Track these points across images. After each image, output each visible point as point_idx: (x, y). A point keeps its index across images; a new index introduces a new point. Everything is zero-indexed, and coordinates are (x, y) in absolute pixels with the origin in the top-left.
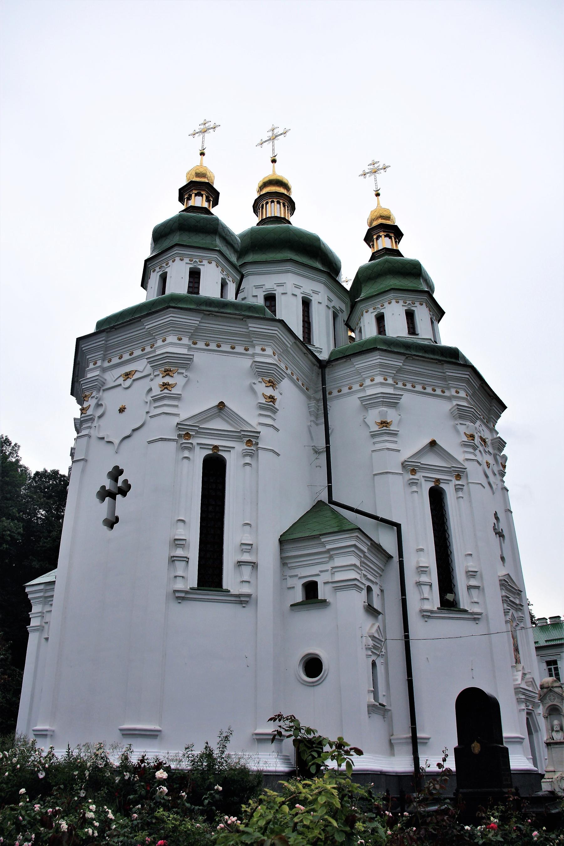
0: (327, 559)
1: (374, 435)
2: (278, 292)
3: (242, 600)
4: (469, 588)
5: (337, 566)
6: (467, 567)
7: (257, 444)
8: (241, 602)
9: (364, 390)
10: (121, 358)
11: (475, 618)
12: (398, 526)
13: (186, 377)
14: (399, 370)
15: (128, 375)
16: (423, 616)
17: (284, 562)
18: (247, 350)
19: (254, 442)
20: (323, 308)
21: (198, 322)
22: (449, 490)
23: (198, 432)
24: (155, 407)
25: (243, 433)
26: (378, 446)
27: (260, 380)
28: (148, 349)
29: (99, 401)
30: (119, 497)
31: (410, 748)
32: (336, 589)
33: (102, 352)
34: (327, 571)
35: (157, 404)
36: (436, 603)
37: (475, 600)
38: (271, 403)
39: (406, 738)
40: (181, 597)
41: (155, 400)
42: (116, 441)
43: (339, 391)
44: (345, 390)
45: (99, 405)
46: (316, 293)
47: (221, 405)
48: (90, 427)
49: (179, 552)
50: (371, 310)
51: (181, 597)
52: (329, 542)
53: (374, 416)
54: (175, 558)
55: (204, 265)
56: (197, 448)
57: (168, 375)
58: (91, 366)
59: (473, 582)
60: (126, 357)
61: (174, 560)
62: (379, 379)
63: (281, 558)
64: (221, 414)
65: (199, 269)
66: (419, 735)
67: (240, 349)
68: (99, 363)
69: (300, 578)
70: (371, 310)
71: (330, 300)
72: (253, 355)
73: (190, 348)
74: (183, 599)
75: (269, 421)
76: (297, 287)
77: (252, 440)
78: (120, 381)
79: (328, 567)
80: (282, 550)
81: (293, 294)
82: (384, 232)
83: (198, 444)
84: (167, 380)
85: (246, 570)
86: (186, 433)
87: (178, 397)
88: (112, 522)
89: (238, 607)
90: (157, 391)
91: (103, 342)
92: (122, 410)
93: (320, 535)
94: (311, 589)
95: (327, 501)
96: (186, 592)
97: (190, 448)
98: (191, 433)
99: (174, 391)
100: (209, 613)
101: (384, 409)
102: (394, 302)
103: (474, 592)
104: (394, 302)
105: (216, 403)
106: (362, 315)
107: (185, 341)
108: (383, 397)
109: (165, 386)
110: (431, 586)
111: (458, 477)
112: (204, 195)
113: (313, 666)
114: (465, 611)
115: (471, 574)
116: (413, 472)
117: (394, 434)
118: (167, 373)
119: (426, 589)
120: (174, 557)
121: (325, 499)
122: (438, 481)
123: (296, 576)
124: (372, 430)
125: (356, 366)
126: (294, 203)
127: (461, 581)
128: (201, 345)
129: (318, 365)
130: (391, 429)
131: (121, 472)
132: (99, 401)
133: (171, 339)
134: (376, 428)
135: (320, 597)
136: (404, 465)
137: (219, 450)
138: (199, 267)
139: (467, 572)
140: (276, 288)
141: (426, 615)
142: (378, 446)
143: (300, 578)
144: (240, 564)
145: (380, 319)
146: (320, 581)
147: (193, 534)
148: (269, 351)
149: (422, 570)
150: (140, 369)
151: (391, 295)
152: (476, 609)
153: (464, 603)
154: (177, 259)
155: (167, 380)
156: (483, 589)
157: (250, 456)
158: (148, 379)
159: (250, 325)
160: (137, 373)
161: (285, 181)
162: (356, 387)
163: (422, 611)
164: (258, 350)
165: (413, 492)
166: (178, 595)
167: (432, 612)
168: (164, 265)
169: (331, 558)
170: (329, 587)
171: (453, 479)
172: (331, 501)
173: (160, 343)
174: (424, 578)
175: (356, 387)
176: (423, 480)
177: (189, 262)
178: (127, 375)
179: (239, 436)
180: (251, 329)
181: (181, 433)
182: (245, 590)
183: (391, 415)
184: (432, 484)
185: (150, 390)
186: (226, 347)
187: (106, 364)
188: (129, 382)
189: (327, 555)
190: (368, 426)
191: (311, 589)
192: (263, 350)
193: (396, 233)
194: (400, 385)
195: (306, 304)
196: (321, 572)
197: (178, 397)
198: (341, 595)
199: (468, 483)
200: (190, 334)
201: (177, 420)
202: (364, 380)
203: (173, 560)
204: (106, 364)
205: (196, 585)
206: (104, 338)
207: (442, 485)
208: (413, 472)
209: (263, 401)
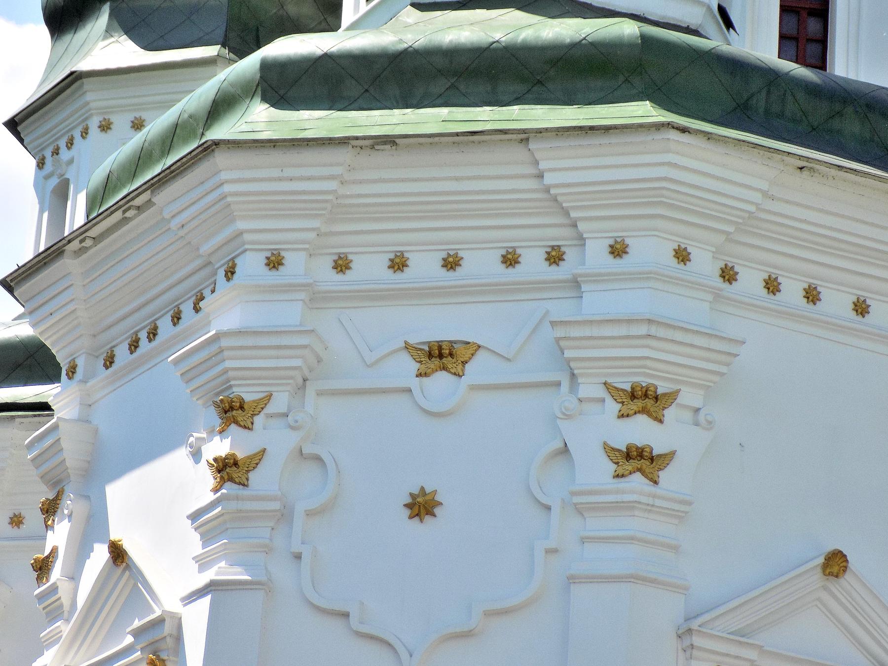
15: (441, 356)
21: (757, 197)
35: (597, 525)
47: (835, 563)
60: (425, 266)
64: (825, 596)
84: (640, 431)
90: (597, 471)
91: (333, 185)
92: (422, 507)
107: (705, 264)
109: (639, 459)
118: (644, 400)
155: (640, 431)
160: (481, 355)
178: (440, 356)
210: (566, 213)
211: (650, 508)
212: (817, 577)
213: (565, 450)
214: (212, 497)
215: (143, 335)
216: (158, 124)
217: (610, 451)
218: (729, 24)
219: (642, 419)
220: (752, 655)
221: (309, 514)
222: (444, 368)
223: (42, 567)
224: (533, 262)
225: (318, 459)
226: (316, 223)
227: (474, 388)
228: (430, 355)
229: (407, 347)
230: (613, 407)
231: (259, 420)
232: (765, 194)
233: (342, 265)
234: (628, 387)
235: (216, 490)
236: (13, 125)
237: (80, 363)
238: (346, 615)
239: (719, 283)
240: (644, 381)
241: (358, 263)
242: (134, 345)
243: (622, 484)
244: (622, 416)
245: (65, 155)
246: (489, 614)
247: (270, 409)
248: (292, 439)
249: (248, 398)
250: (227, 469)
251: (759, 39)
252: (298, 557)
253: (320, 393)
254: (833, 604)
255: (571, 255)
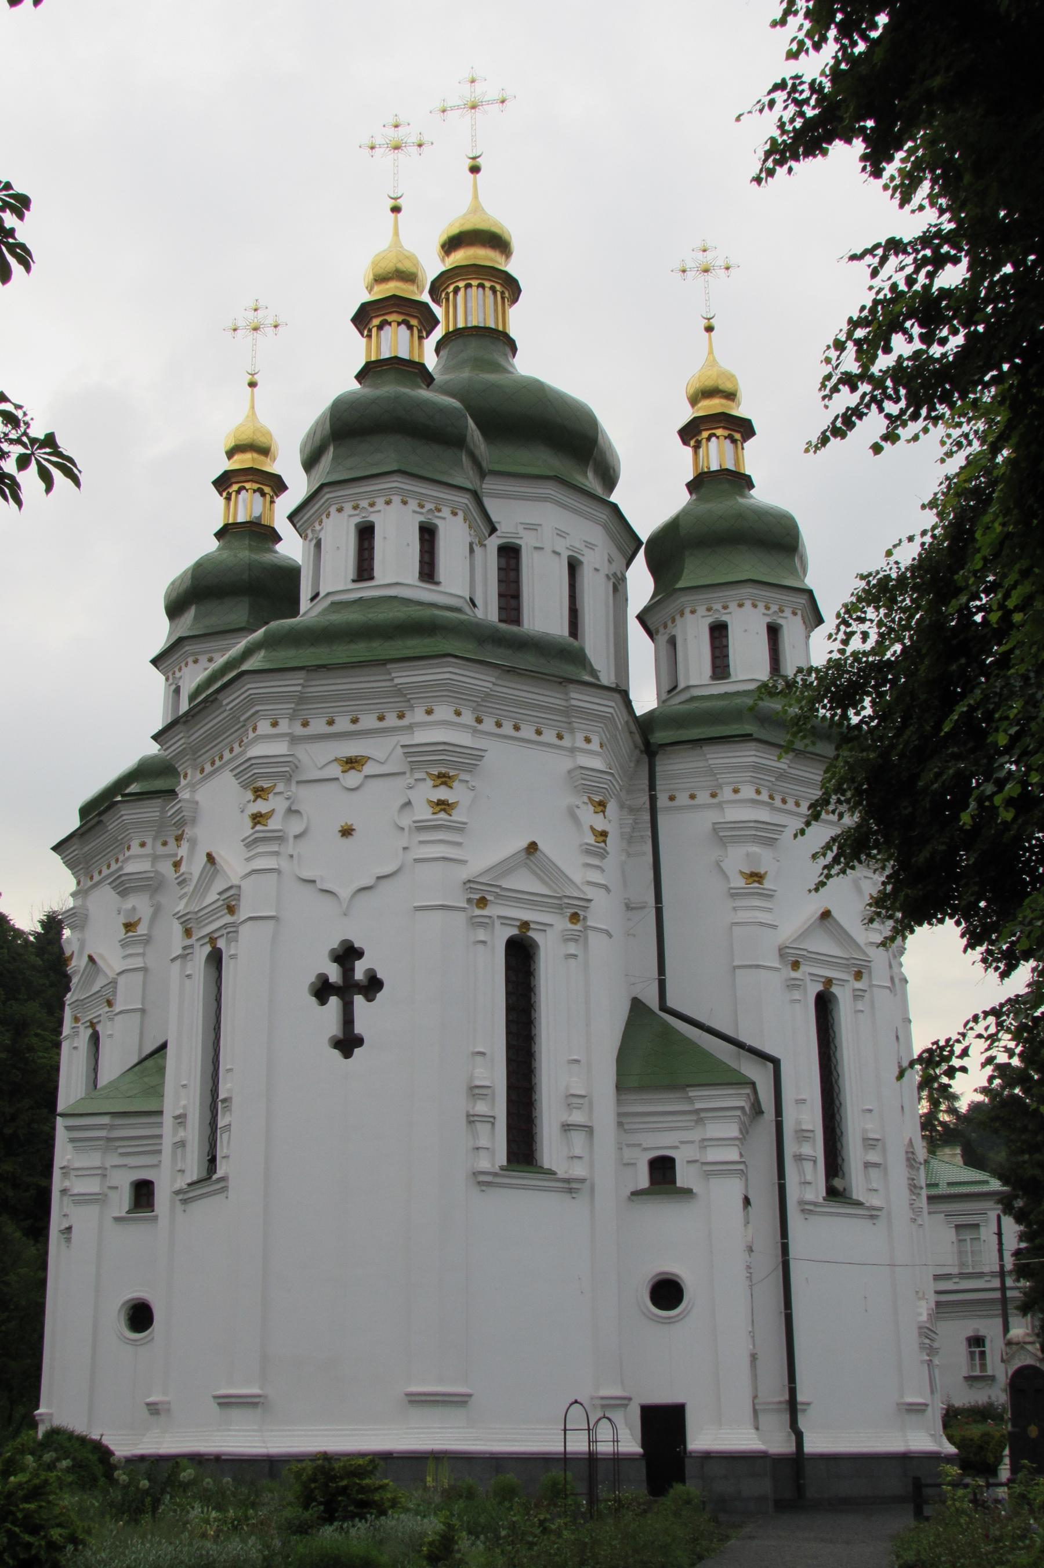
0: (693, 1124)
1: (734, 895)
2: (527, 542)
3: (570, 1187)
4: (867, 1165)
5: (706, 1136)
6: (865, 1131)
7: (585, 918)
8: (570, 1191)
9: (720, 806)
10: (331, 723)
11: (873, 1214)
12: (776, 1062)
13: (473, 789)
14: (782, 776)
15: (351, 762)
16: (803, 1210)
17: (622, 1122)
18: (560, 737)
19: (582, 917)
20: (601, 579)
22: (843, 994)
23: (498, 896)
24: (421, 842)
25: (566, 901)
26: (742, 916)
27: (586, 800)
28: (392, 720)
29: (292, 803)
30: (359, 1000)
31: (786, 1417)
32: (708, 1174)
33: (292, 706)
34: (692, 1142)
36: (823, 1192)
37: (875, 1186)
38: (603, 845)
39: (780, 1403)
40: (482, 1181)
41: (420, 829)
42: (345, 893)
43: (672, 798)
44: (683, 799)
45: (292, 812)
46: (590, 546)
47: (532, 848)
48: (277, 853)
49: (481, 1108)
50: (701, 610)
51: (482, 1181)
52: (701, 1098)
53: (737, 859)
54: (476, 1118)
55: (444, 518)
56: (497, 923)
57: (444, 783)
58: (264, 727)
59: (873, 1157)
60: (343, 724)
61: (473, 1121)
62: (748, 792)
63: (619, 1115)
64: (528, 861)
65: (436, 526)
66: (800, 1398)
67: (549, 736)
68: (284, 726)
69: (645, 1149)
70: (701, 610)
71: (610, 561)
72: (573, 750)
73: (475, 731)
74: (488, 1184)
75: (596, 877)
76: (561, 534)
77: (579, 912)
78: (335, 770)
79: (696, 1135)
80: (619, 1102)
81: (554, 552)
82: (724, 428)
83: (499, 917)
84: (442, 793)
85: (578, 1139)
86: (480, 897)
87: (460, 828)
88: (348, 1043)
89: (567, 1197)
90: (423, 813)
91: (299, 688)
92: (347, 832)
93: (688, 1086)
94: (662, 1170)
95: (654, 1003)
96: (495, 1175)
97: (485, 924)
98: (489, 898)
99: (458, 816)
100: (524, 1205)
101: (755, 849)
102: (748, 604)
103: (874, 1173)
104: (748, 604)
105: (524, 844)
106: (682, 614)
107: (468, 718)
108: (757, 829)
109: (443, 806)
110: (815, 1162)
111: (858, 976)
112: (415, 329)
113: (667, 1293)
114: (859, 1204)
115: (870, 1143)
116: (796, 965)
117: (769, 896)
118: (444, 779)
119: (808, 1166)
120: (473, 1116)
121: (652, 1000)
122: (829, 982)
123: (640, 1145)
124: (732, 885)
125: (711, 762)
126: (519, 291)
127: (854, 1154)
128: (489, 725)
129: (643, 748)
130: (765, 886)
131: (359, 954)
132: (292, 803)
133: (443, 712)
134: (739, 882)
135: (679, 1184)
136: (782, 952)
137: (528, 929)
138: (437, 521)
139: (865, 1140)
140: (522, 533)
141: (807, 1209)
142: (742, 916)
143: (645, 1149)
144: (567, 1127)
145: (719, 631)
146: (680, 1157)
147: (495, 1074)
148: (595, 746)
149: (803, 1135)
150: (380, 755)
151: (747, 590)
152: (875, 1201)
153: (858, 1192)
154: (396, 500)
155: (442, 793)
156: (886, 1169)
157: (576, 941)
158: (401, 782)
159: (573, 695)
160: (370, 763)
161: (506, 236)
162: (703, 797)
163: (802, 1202)
164: (580, 737)
165: (794, 1001)
166: (482, 1178)
167: (815, 1204)
168: (364, 504)
169: (700, 1121)
170: (694, 1169)
171: (851, 978)
172: (664, 1008)
173: (418, 715)
174: (806, 1150)
175: (703, 797)
176: (808, 978)
177: (418, 509)
178: (352, 763)
179: (557, 904)
180: (574, 702)
181: (472, 896)
182: (578, 1170)
183: (765, 860)
184: (820, 987)
185: (409, 803)
186: (527, 732)
187: (299, 730)
188: (353, 778)
189: (694, 1118)
190: (726, 877)
191: (662, 1170)
192: (588, 740)
193: (743, 429)
194: (778, 802)
195: (574, 567)
196: (682, 1142)
197: (460, 828)
198: (715, 1183)
199: (871, 986)
200: (474, 704)
201: (465, 873)
202: (720, 786)
203: (472, 1119)
204: (299, 730)
205: (505, 1163)
206: (301, 681)
207: (834, 989)
208: (796, 965)
209: (591, 839)
210: (405, 695)
211: (448, 827)
212: (523, 855)
213: (409, 803)
214: (252, 831)
215: (217, 759)
216: (220, 660)
217: (430, 802)
218: (474, 605)
219: (443, 787)
220: (497, 890)
221: (296, 837)
222: (353, 768)
223: (177, 865)
224: (392, 720)
225: (297, 812)
226: (292, 706)
227: (366, 777)
228: (347, 763)
229: (336, 760)
230: (430, 783)
231: (271, 796)
232: (494, 684)
233: (305, 724)
234: (436, 773)
235: (253, 828)
236: (155, 662)
237: (189, 772)
238: (314, 882)
239: (476, 724)
240: (443, 770)
241: (312, 722)
242: (213, 763)
243: (435, 817)
244: (434, 786)
245: (178, 675)
246: (379, 878)
247: (276, 790)
248: (286, 804)
249: (265, 786)
250: (258, 818)
251: (488, 611)
252: (292, 856)
253: (298, 782)
254: (533, 866)
255: (408, 714)
